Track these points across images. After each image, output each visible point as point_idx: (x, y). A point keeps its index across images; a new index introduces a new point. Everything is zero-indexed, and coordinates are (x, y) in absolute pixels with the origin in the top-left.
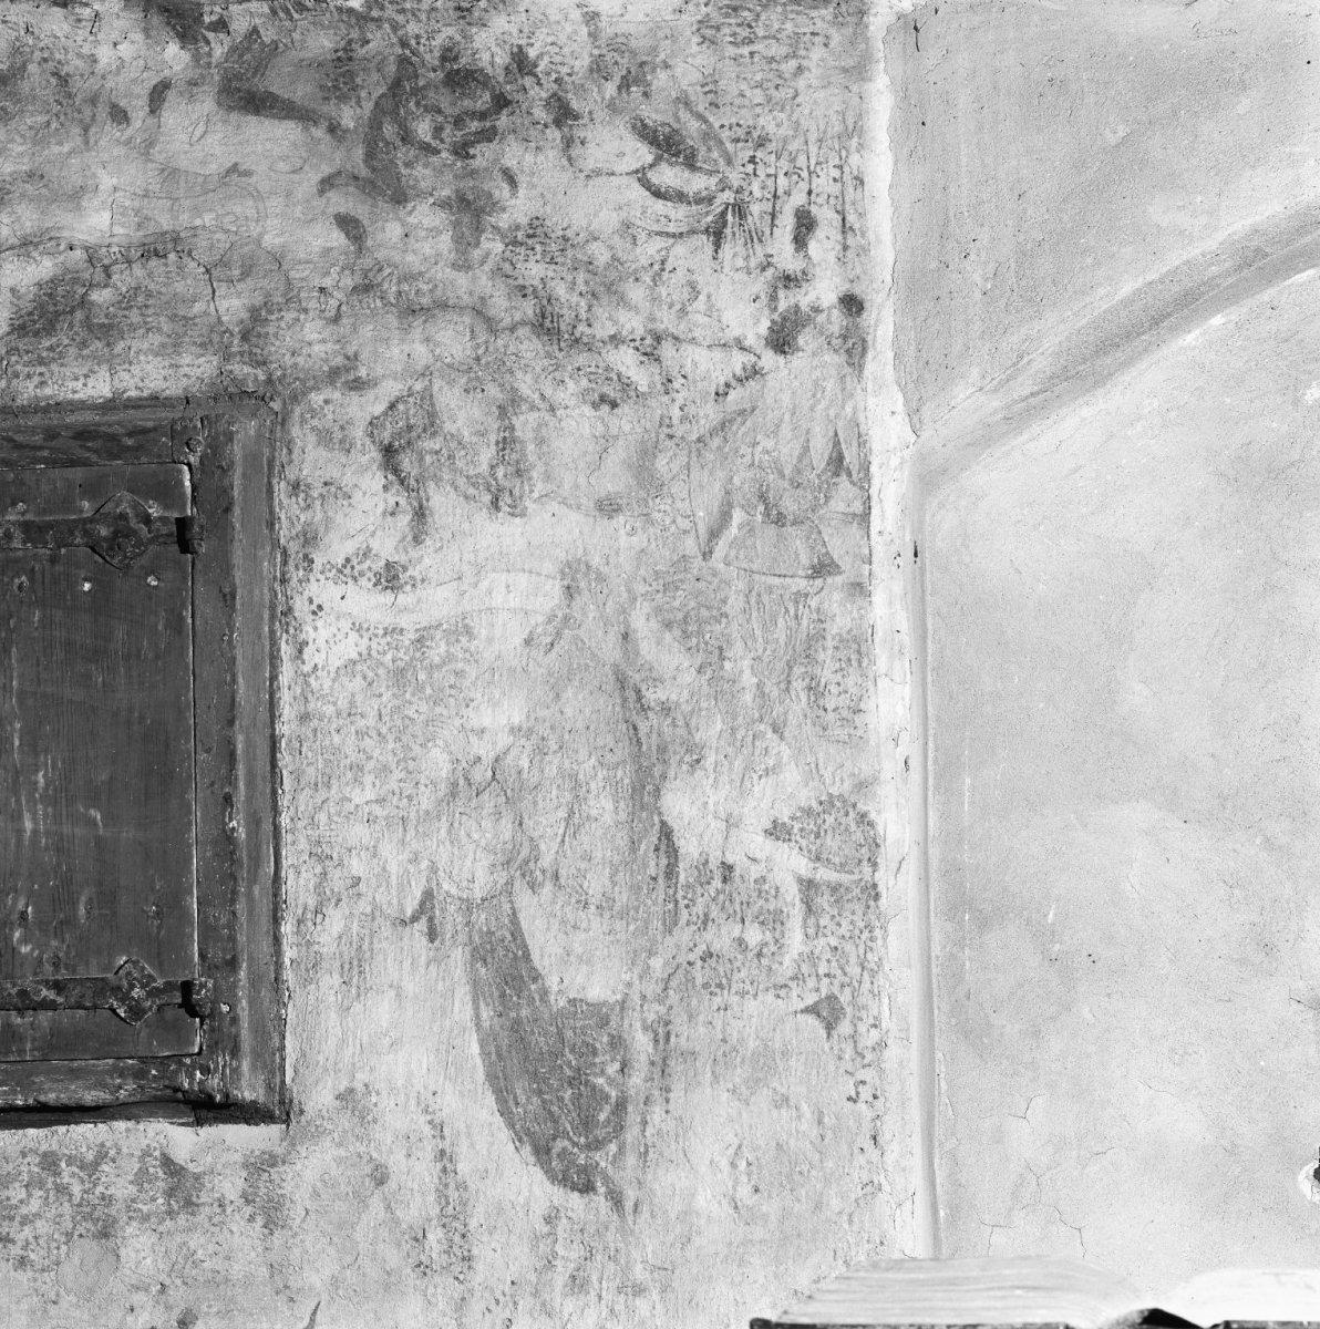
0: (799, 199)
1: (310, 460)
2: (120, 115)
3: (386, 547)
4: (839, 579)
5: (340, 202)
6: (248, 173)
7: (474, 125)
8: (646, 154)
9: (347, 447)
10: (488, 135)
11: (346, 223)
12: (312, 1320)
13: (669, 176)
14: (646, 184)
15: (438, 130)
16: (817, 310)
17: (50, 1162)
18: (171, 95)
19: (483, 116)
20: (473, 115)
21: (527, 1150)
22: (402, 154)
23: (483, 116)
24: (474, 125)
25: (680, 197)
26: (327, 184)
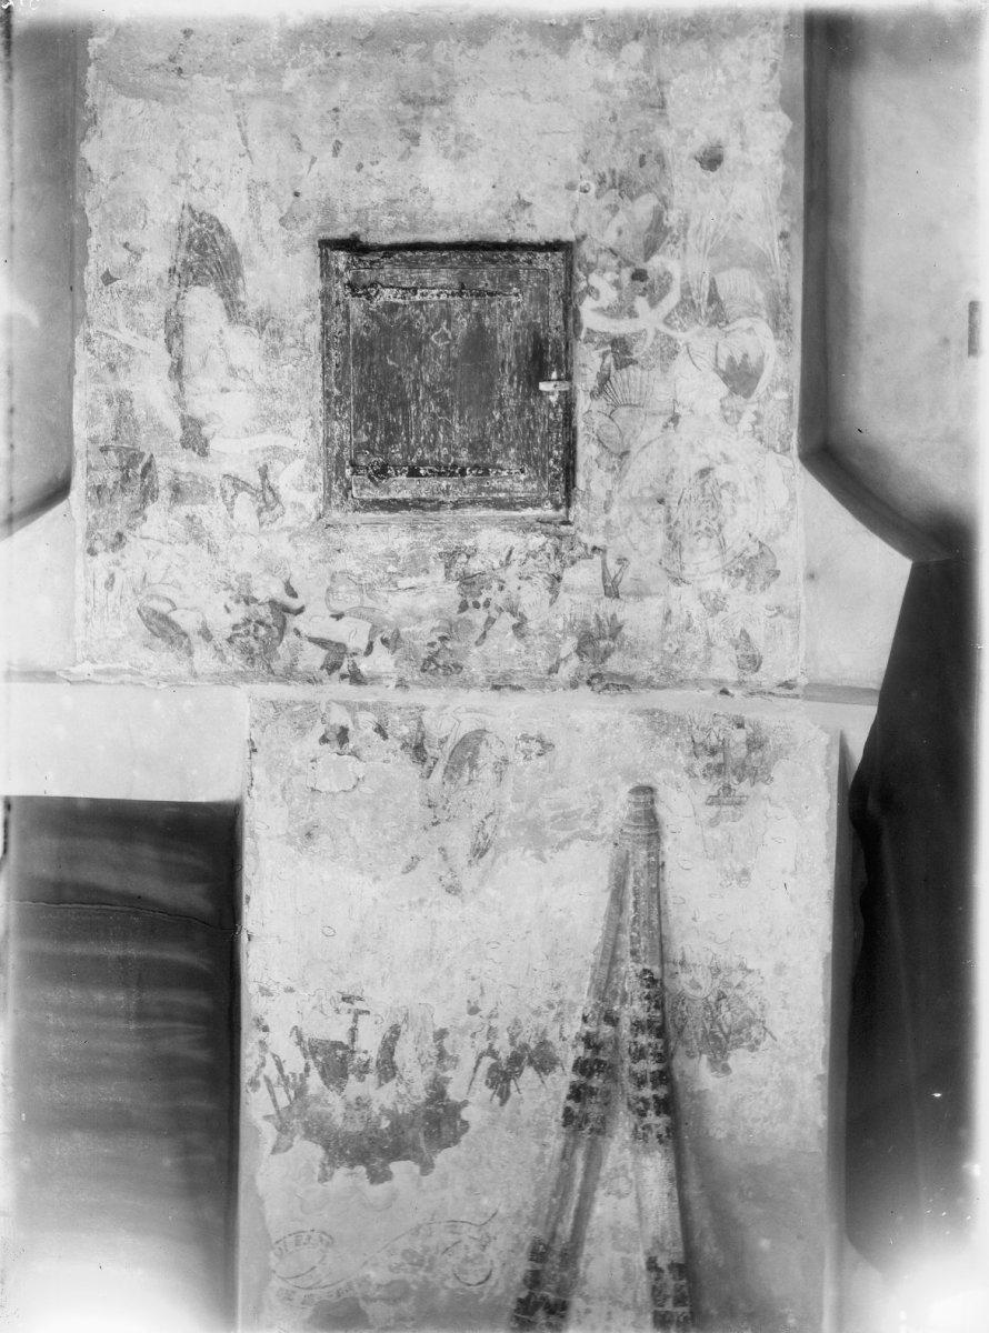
0: (111, 596)
1: (311, 501)
2: (384, 641)
3: (278, 465)
4: (100, 445)
5: (295, 604)
6: (332, 616)
7: (241, 631)
8: (174, 616)
9: (294, 504)
10: (235, 627)
11: (294, 595)
12: (310, 167)
13: (164, 608)
14: (171, 601)
15: (256, 630)
16: (106, 550)
17: (414, 229)
18: (364, 648)
19: (238, 635)
20: (242, 636)
21: (226, 229)
22: (270, 621)
23: (238, 635)
24: (241, 631)
25: (158, 598)
26: (301, 611)
